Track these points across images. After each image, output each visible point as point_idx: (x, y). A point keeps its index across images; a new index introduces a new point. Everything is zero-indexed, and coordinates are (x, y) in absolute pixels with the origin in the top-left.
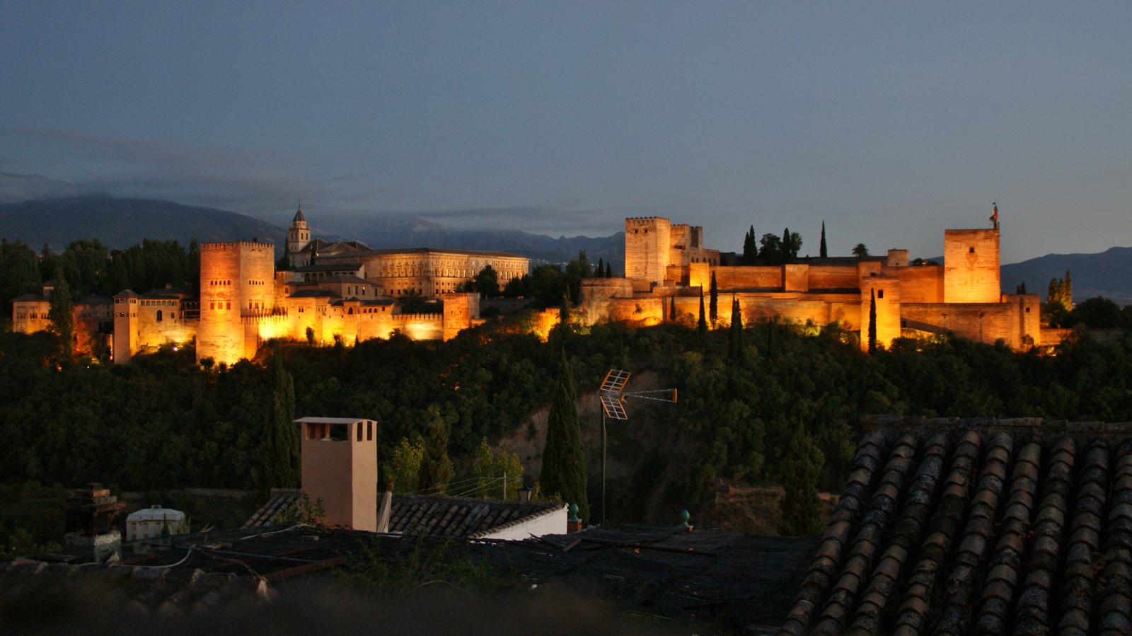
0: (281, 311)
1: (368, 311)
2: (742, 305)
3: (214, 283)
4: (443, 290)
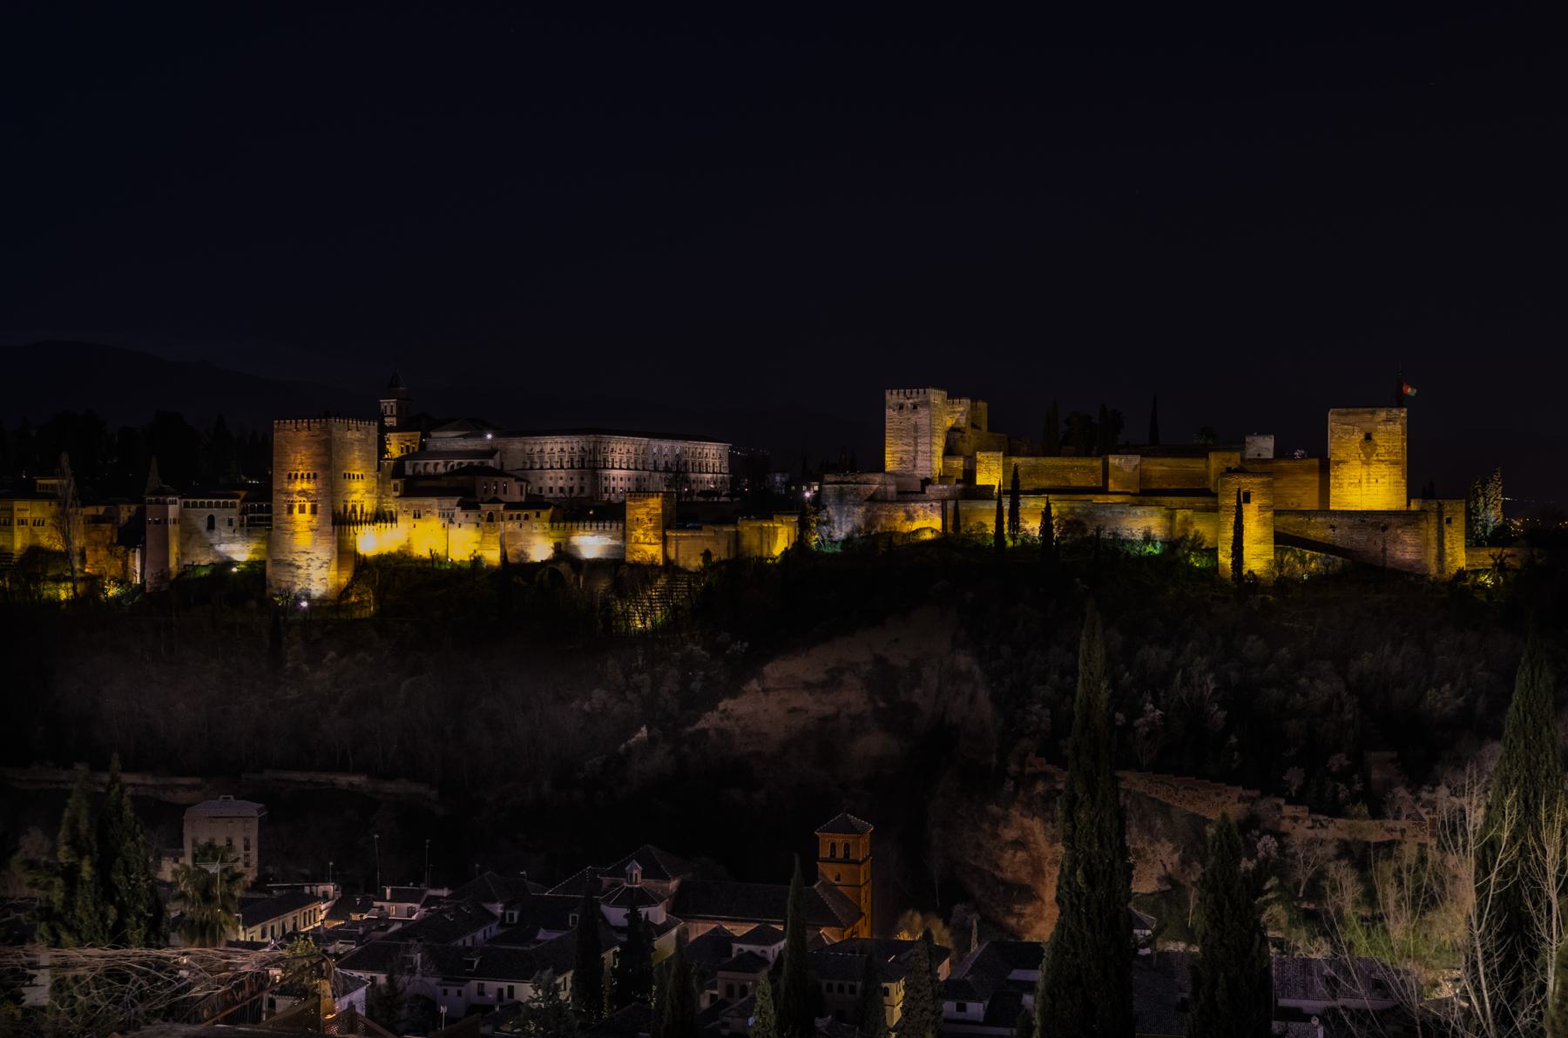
0: (388, 517)
1: (515, 517)
2: (1054, 512)
3: (293, 477)
4: (614, 488)
